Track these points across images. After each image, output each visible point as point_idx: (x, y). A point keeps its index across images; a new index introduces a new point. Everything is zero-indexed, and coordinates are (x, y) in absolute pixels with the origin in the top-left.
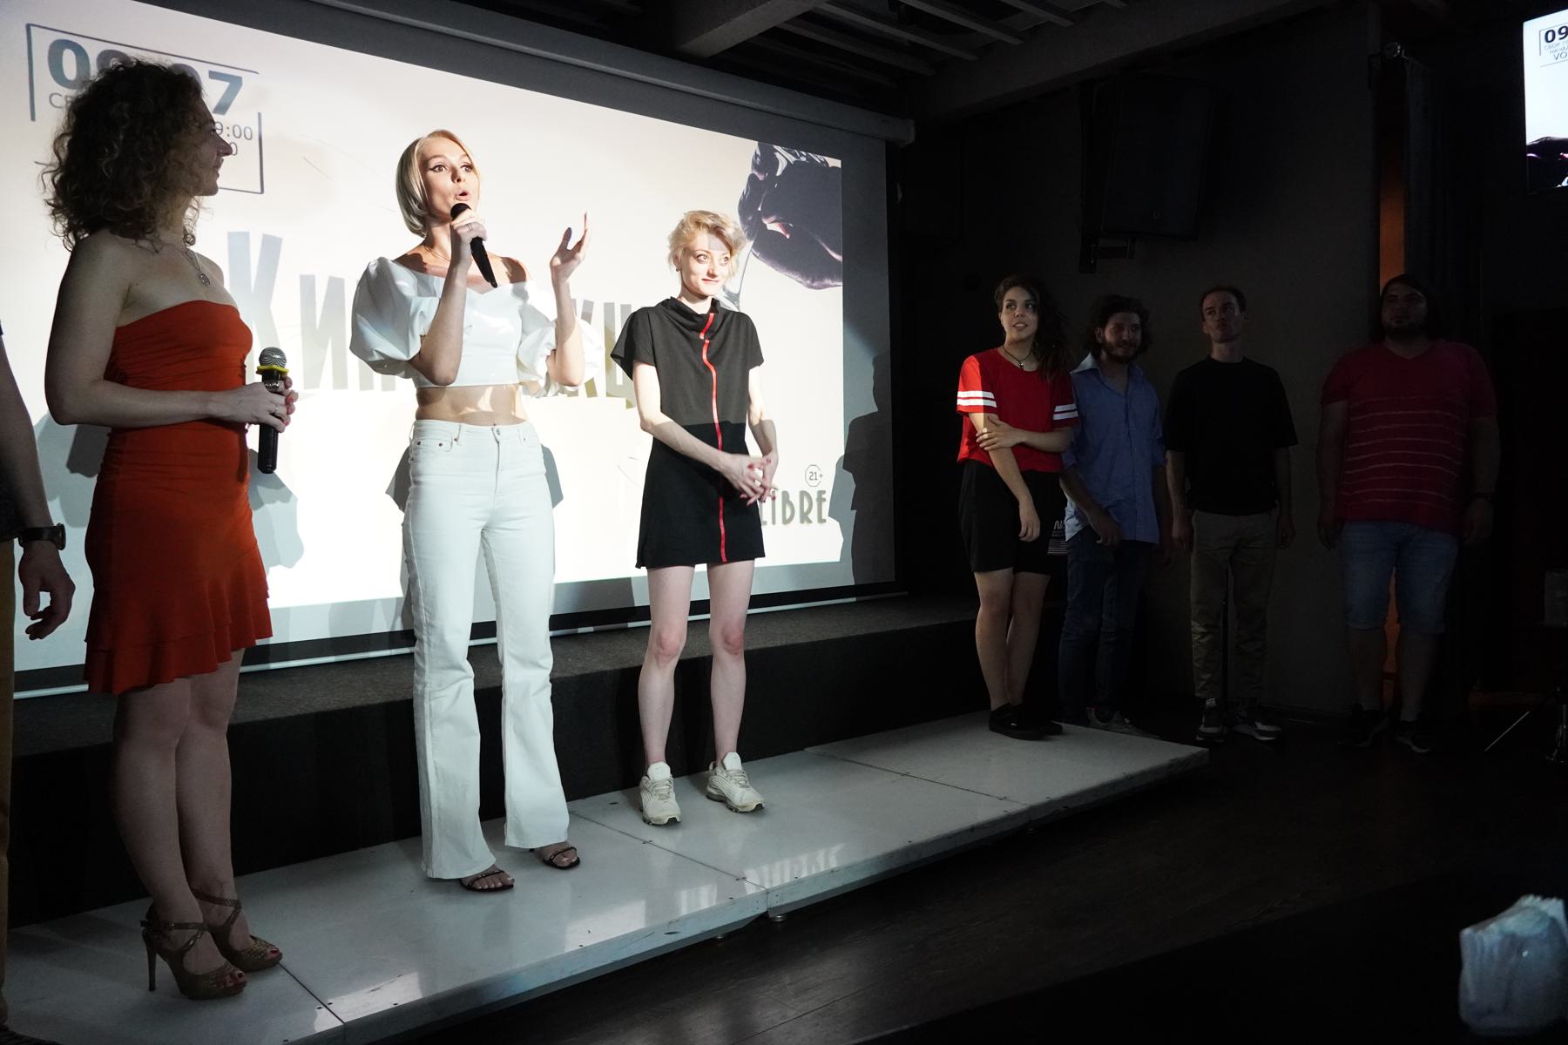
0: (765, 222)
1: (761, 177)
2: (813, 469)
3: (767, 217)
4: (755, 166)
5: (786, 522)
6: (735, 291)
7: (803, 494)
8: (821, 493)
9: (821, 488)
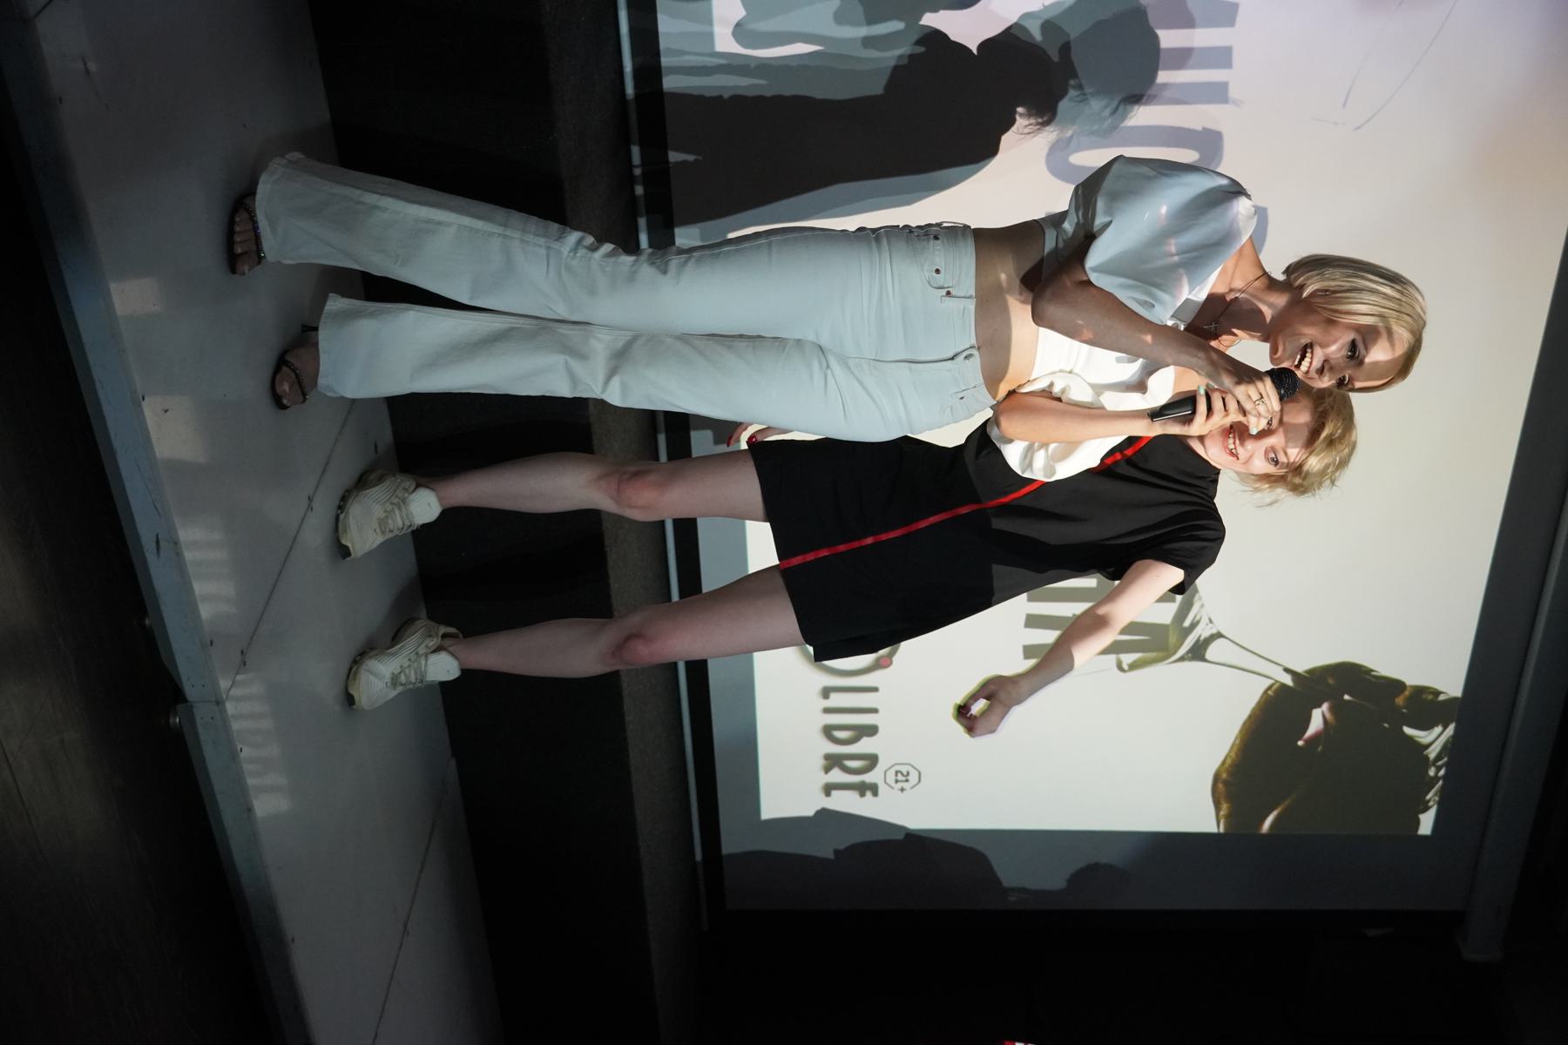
0: (1325, 706)
1: (1400, 701)
2: (913, 778)
3: (1331, 709)
4: (1420, 691)
5: (828, 731)
6: (1212, 652)
7: (872, 761)
8: (874, 789)
9: (882, 788)
